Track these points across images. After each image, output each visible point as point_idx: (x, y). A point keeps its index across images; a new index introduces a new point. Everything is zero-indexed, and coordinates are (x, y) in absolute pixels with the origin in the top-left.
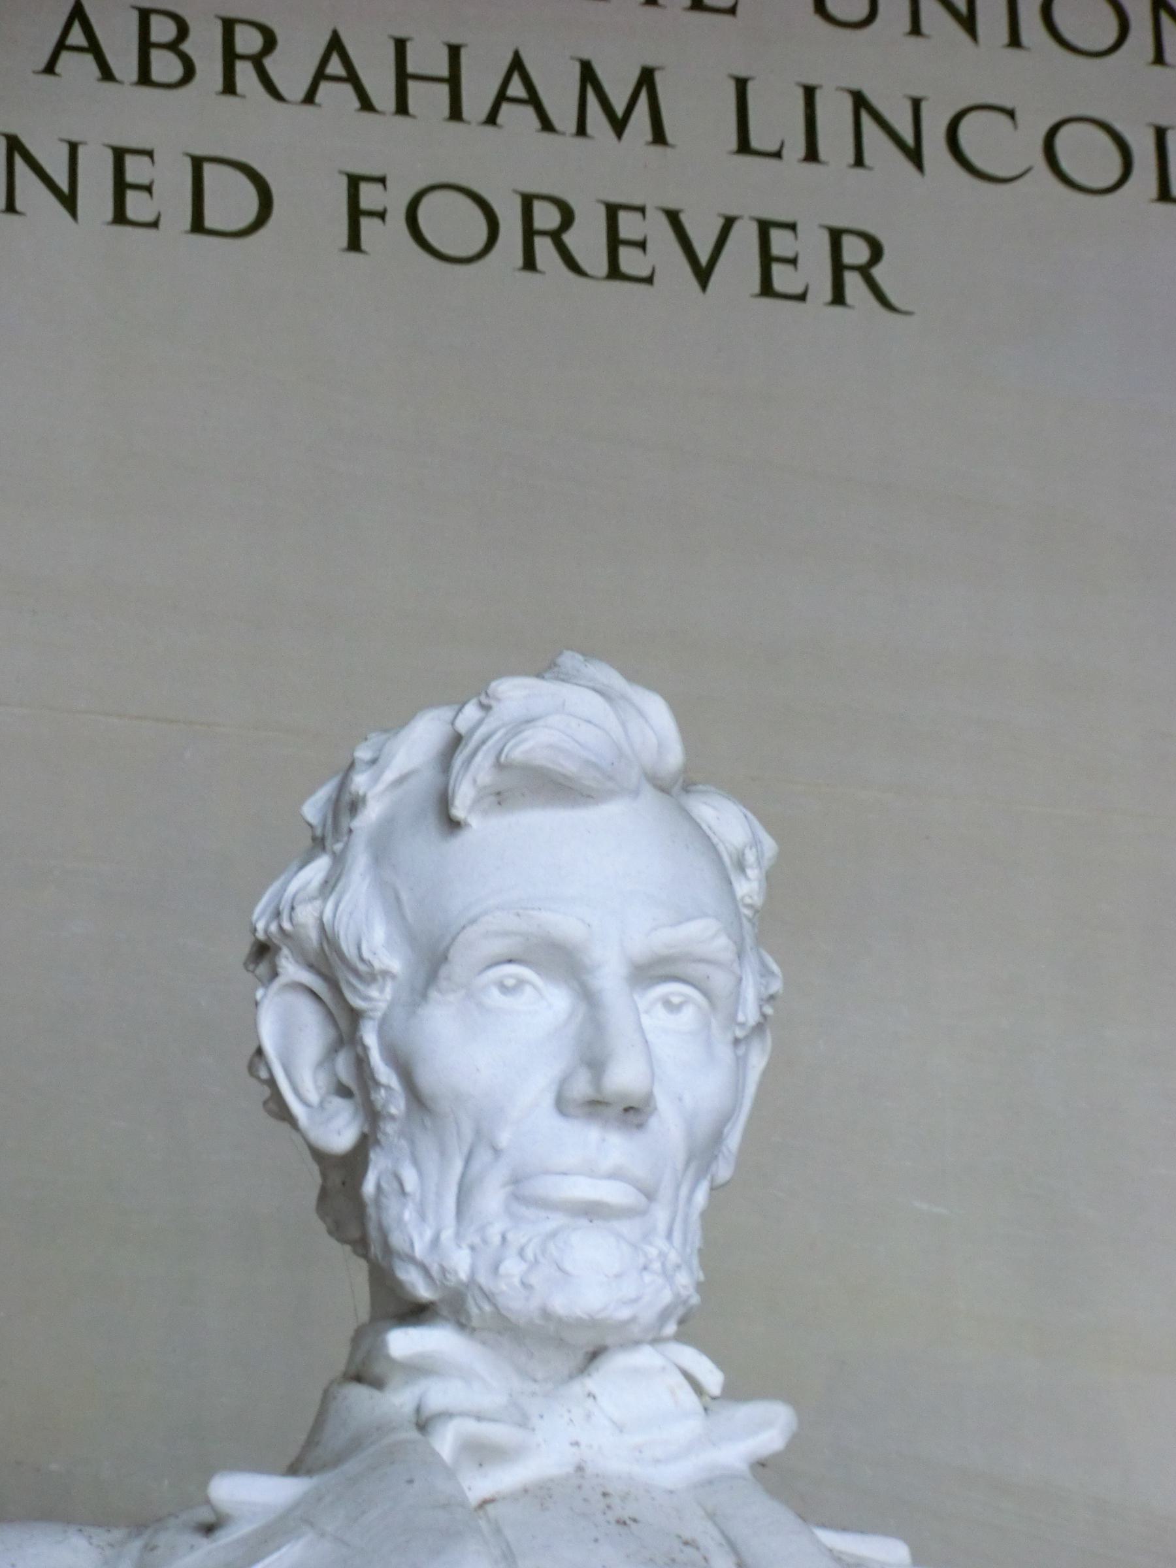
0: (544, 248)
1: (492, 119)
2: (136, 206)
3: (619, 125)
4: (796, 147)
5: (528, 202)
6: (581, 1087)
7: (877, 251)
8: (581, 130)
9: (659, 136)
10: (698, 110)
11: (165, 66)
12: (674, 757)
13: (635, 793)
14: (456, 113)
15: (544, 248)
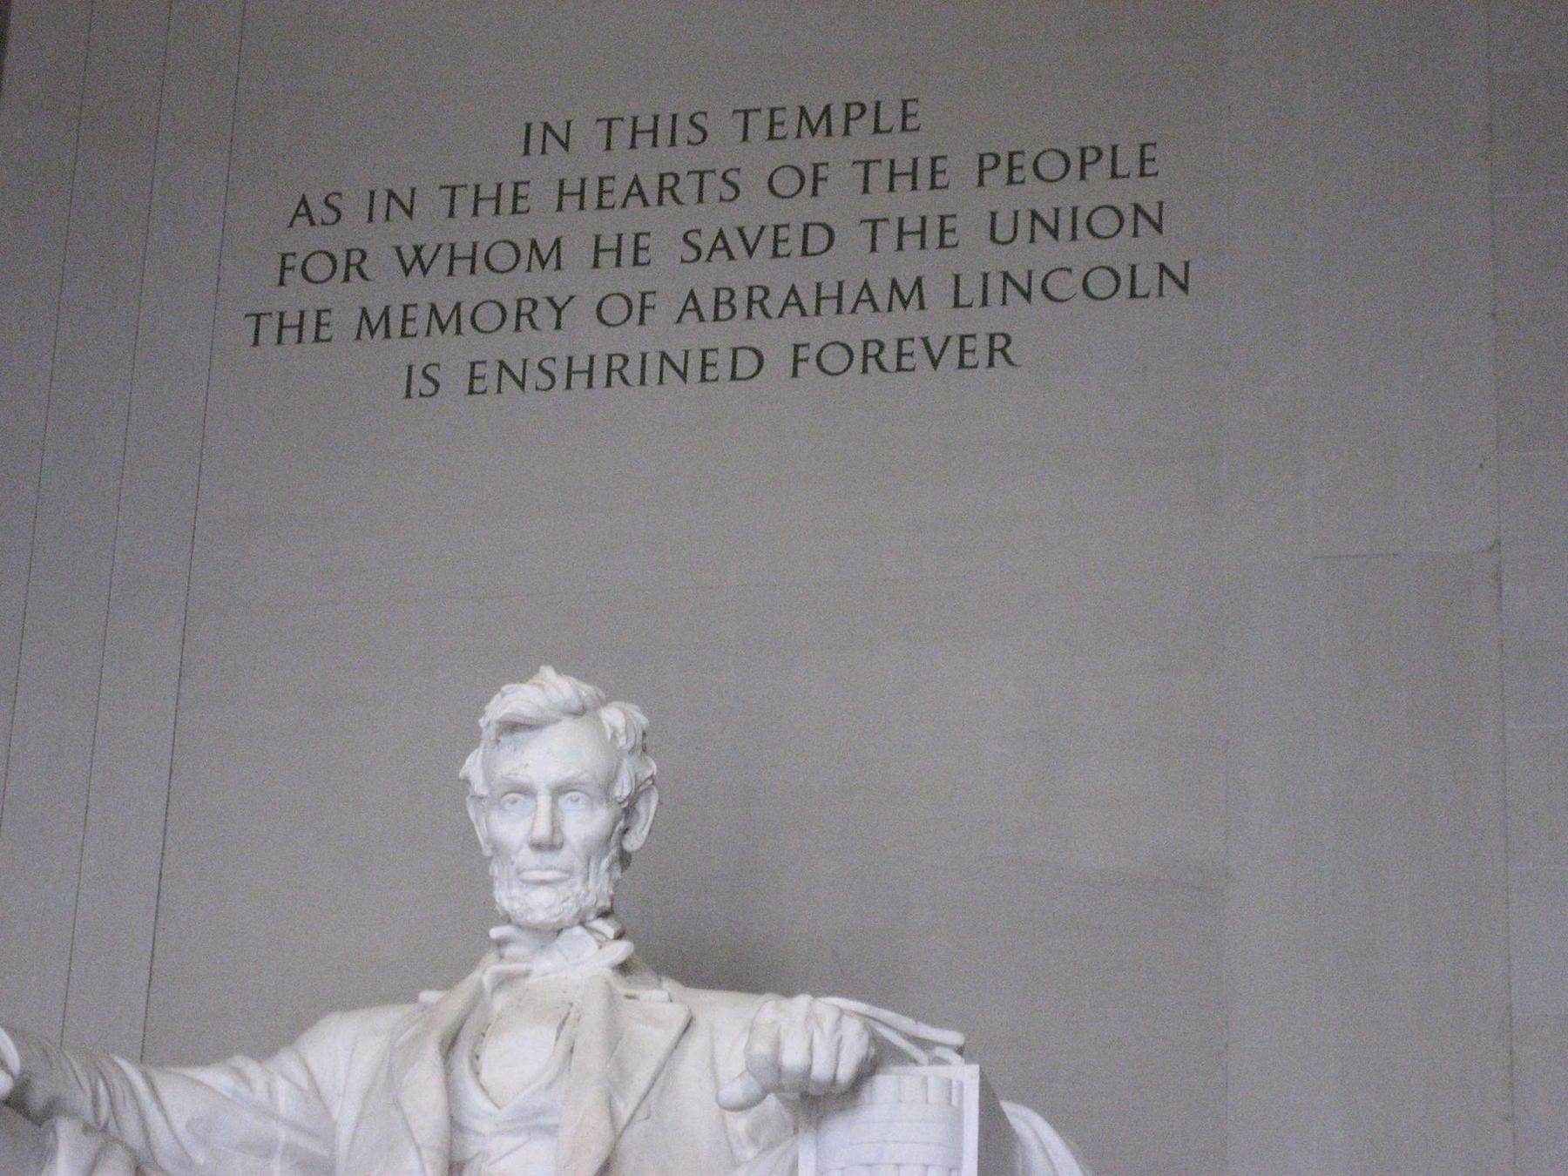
0: (872, 363)
1: (853, 311)
2: (710, 373)
4: (978, 301)
5: (866, 344)
7: (1008, 342)
8: (890, 309)
9: (922, 306)
10: (938, 292)
11: (725, 311)
13: (558, 721)
14: (839, 311)
15: (872, 363)
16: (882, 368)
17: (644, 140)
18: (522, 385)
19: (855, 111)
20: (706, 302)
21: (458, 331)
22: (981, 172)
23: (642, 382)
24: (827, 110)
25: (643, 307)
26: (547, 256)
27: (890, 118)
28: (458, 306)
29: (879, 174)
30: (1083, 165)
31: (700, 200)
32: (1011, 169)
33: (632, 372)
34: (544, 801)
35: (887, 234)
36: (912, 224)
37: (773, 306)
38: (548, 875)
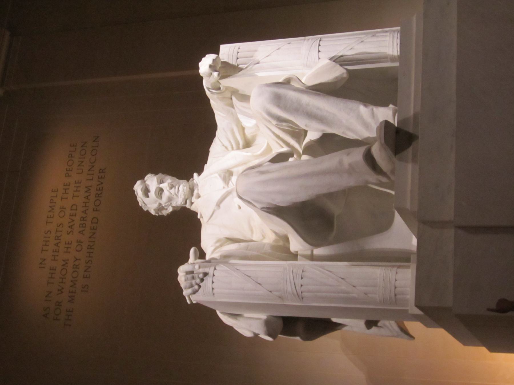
3: (90, 189)
6: (168, 189)
11: (84, 225)
12: (142, 180)
16: (101, 193)
17: (48, 243)
18: (90, 267)
19: (52, 201)
20: (82, 229)
21: (76, 281)
22: (68, 176)
23: (94, 242)
24: (50, 207)
25: (80, 242)
26: (66, 262)
27: (54, 194)
28: (72, 281)
29: (65, 196)
30: (72, 157)
31: (61, 231)
32: (69, 170)
33: (91, 244)
34: (162, 186)
35: (76, 194)
36: (75, 189)
37: (84, 216)
38: (177, 187)
